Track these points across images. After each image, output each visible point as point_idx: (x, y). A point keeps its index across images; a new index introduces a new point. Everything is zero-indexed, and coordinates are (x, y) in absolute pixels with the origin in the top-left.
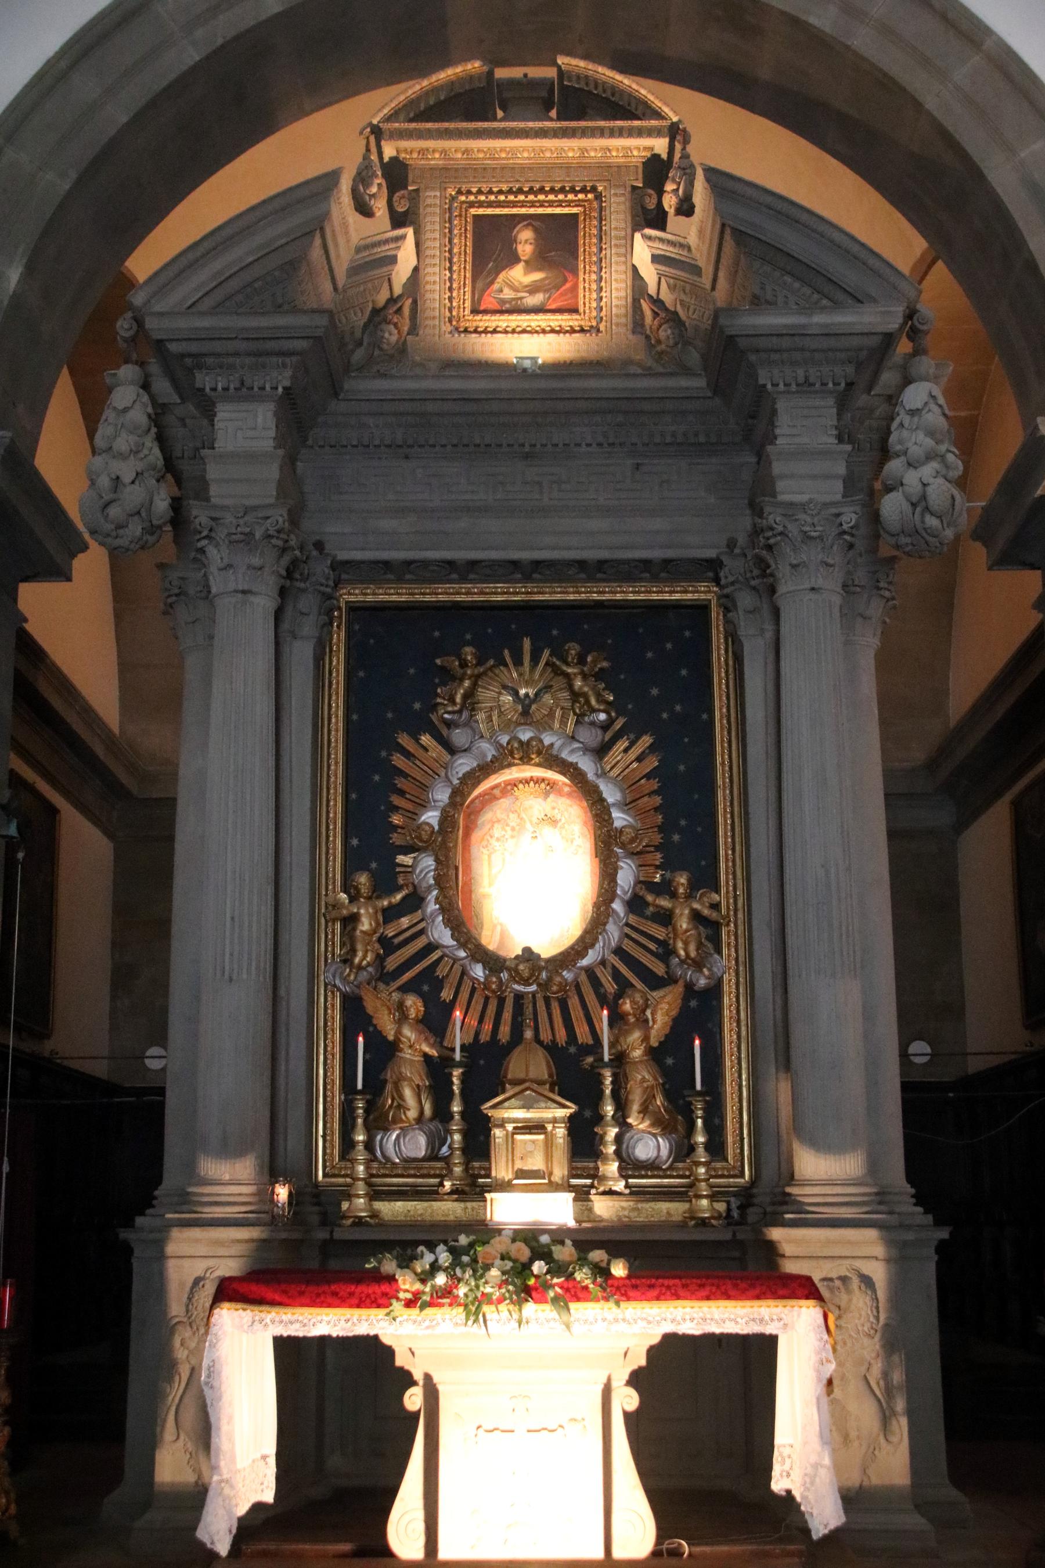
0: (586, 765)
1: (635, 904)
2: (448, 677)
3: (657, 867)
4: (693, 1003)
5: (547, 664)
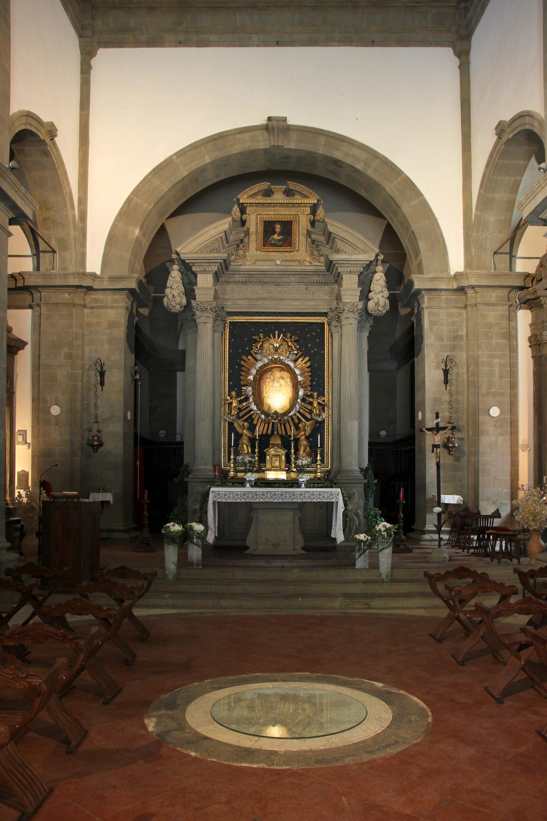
0: (292, 364)
1: (303, 400)
2: (256, 341)
4: (317, 425)
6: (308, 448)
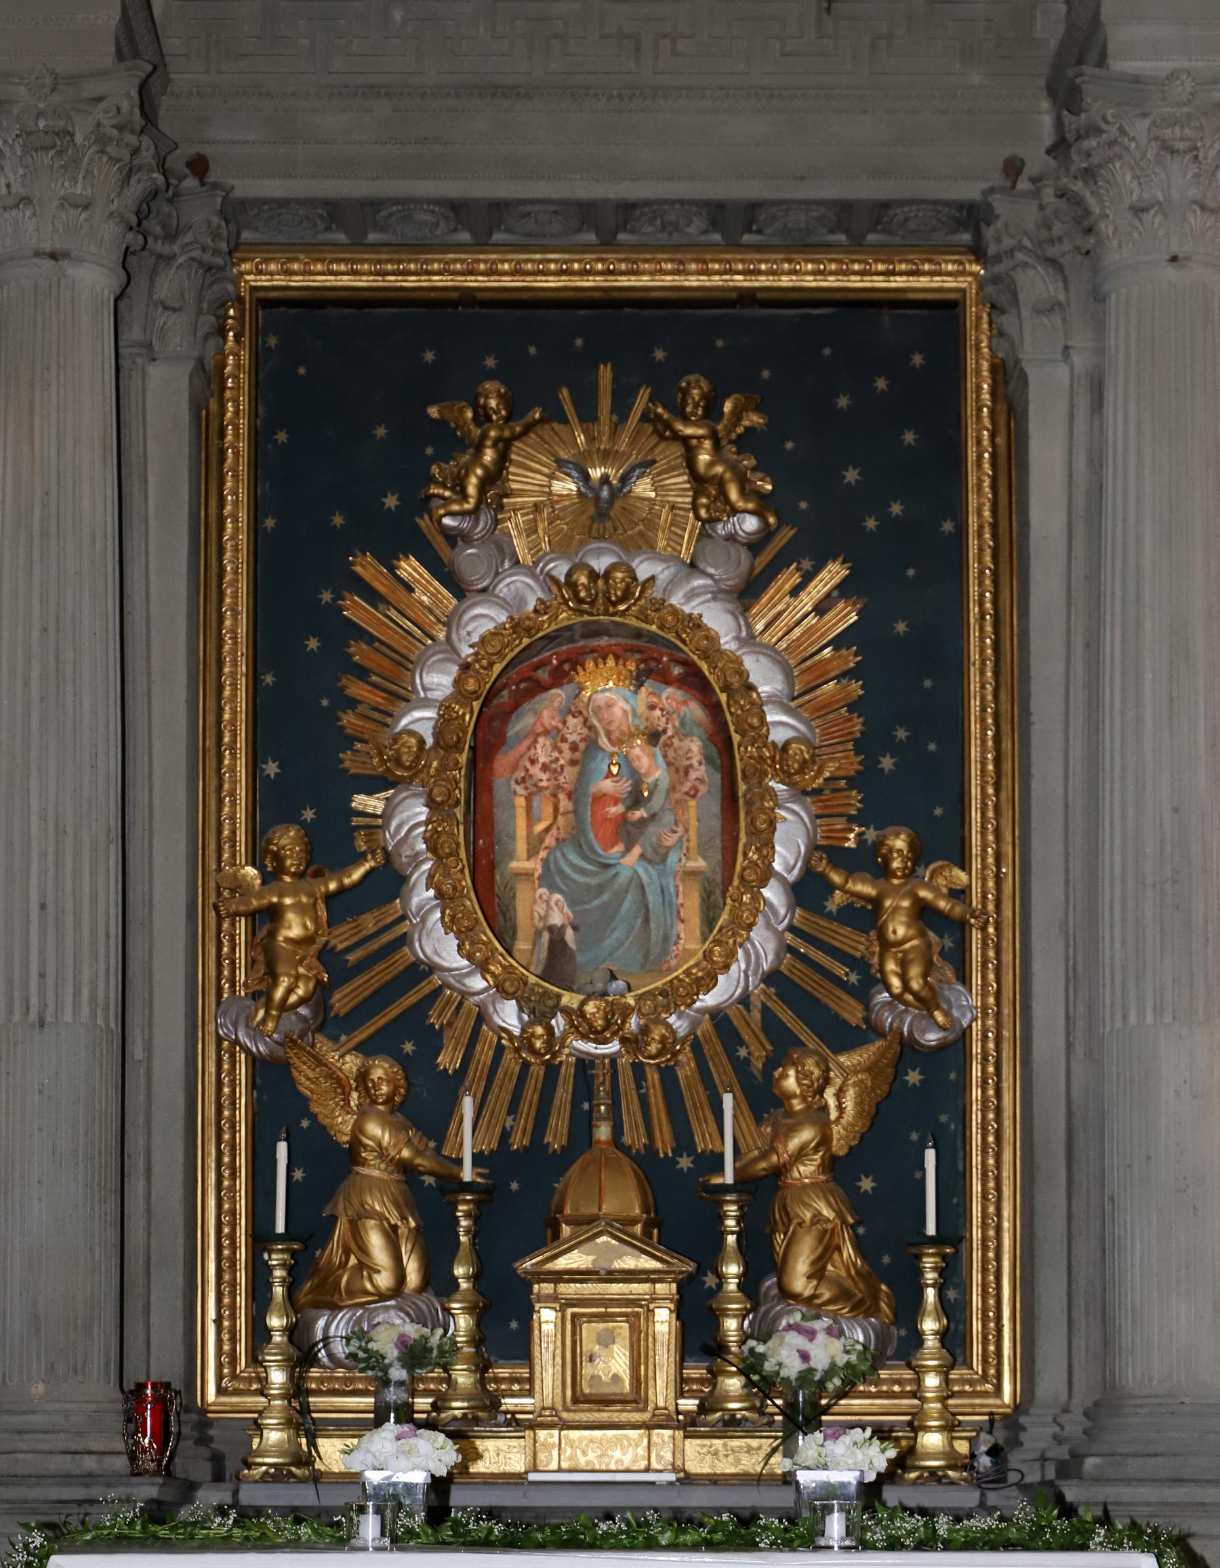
2: (451, 442)
3: (851, 819)
5: (645, 418)
6: (848, 1251)
